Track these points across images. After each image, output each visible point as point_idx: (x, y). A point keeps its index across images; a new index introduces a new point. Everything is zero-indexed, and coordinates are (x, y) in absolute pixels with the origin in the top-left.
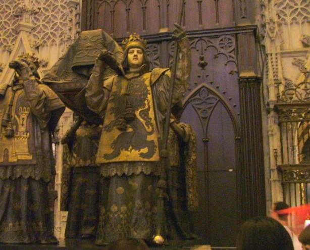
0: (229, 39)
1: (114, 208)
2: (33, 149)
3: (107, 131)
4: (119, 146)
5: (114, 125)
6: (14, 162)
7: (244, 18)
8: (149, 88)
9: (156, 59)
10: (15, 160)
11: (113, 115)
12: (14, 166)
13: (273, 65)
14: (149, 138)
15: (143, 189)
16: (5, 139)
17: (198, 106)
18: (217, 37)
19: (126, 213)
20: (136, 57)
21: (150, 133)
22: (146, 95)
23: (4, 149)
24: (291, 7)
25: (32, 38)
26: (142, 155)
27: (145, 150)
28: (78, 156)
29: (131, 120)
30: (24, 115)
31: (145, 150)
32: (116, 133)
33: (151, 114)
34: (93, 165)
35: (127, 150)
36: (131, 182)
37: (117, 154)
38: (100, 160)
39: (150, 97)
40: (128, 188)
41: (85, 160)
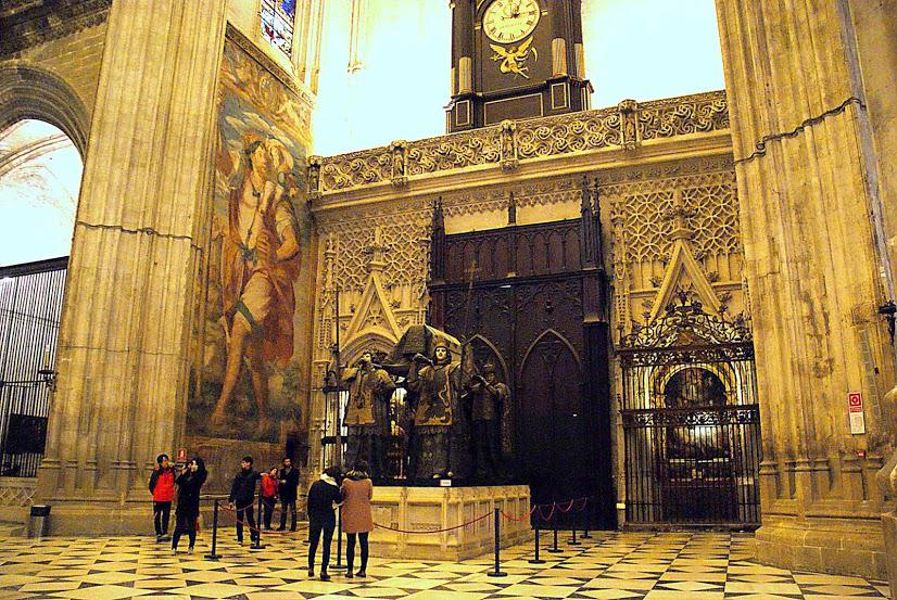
1: (425, 455)
2: (375, 415)
4: (429, 414)
12: (363, 426)
15: (442, 443)
20: (441, 355)
24: (642, 245)
25: (384, 277)
29: (436, 399)
30: (369, 392)
33: (448, 394)
40: (433, 441)
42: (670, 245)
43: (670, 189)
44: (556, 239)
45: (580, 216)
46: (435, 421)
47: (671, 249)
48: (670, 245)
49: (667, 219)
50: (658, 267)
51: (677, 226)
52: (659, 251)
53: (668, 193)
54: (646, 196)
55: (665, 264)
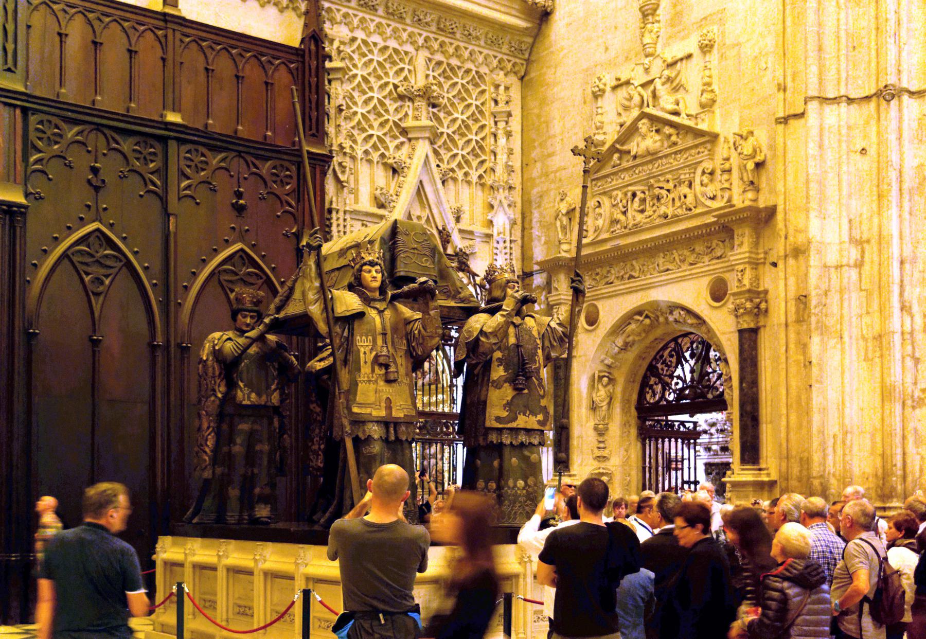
0: (288, 170)
1: (511, 483)
3: (496, 387)
5: (505, 381)
6: (400, 418)
7: (313, 135)
8: (538, 341)
9: (152, 173)
10: (402, 415)
11: (502, 368)
12: (397, 424)
13: (339, 232)
14: (543, 402)
16: (382, 383)
17: (230, 285)
18: (267, 159)
19: (524, 488)
21: (543, 397)
22: (536, 348)
23: (385, 397)
26: (539, 422)
27: (540, 417)
28: (245, 386)
31: (540, 417)
32: (508, 392)
34: (269, 404)
35: (524, 414)
36: (526, 453)
37: (515, 419)
38: (491, 423)
39: (540, 351)
41: (259, 395)
42: (402, 143)
43: (409, 48)
44: (252, 71)
45: (295, 42)
46: (522, 421)
47: (406, 149)
48: (402, 143)
49: (401, 97)
50: (381, 177)
51: (418, 117)
52: (387, 148)
53: (406, 53)
54: (375, 44)
55: (395, 171)
